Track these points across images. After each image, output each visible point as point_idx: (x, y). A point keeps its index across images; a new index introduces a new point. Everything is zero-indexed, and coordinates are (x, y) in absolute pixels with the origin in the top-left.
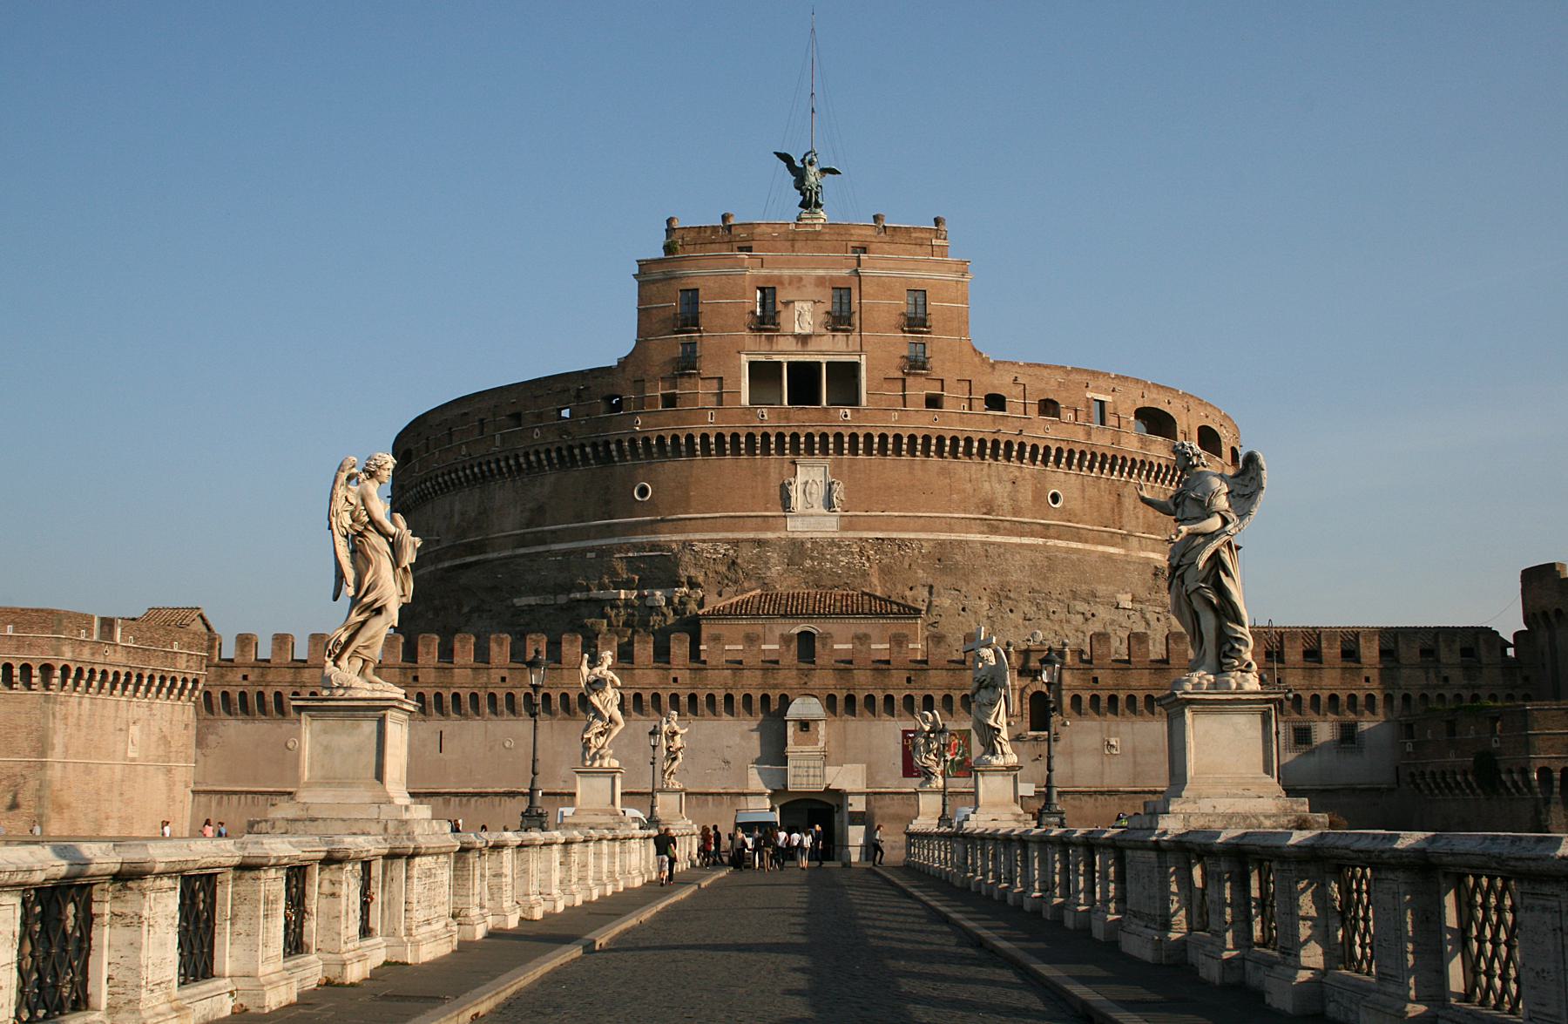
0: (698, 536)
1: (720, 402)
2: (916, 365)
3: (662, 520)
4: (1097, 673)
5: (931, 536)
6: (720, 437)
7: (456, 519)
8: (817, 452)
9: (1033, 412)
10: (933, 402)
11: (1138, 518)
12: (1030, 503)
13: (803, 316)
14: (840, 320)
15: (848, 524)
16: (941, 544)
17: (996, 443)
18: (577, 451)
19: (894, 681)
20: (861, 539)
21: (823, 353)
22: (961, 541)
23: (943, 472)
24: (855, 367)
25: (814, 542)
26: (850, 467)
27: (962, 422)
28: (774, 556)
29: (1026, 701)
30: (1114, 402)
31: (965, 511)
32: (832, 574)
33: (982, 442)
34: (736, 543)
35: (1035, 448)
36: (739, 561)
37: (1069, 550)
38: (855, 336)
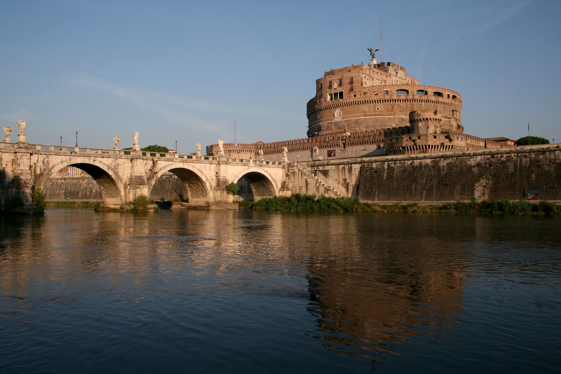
1: (325, 101)
2: (352, 90)
4: (351, 139)
10: (355, 96)
11: (398, 110)
13: (335, 85)
14: (340, 85)
15: (343, 118)
16: (356, 120)
21: (338, 91)
24: (342, 92)
25: (338, 121)
27: (359, 99)
28: (333, 125)
30: (391, 90)
31: (361, 113)
34: (328, 123)
38: (342, 87)
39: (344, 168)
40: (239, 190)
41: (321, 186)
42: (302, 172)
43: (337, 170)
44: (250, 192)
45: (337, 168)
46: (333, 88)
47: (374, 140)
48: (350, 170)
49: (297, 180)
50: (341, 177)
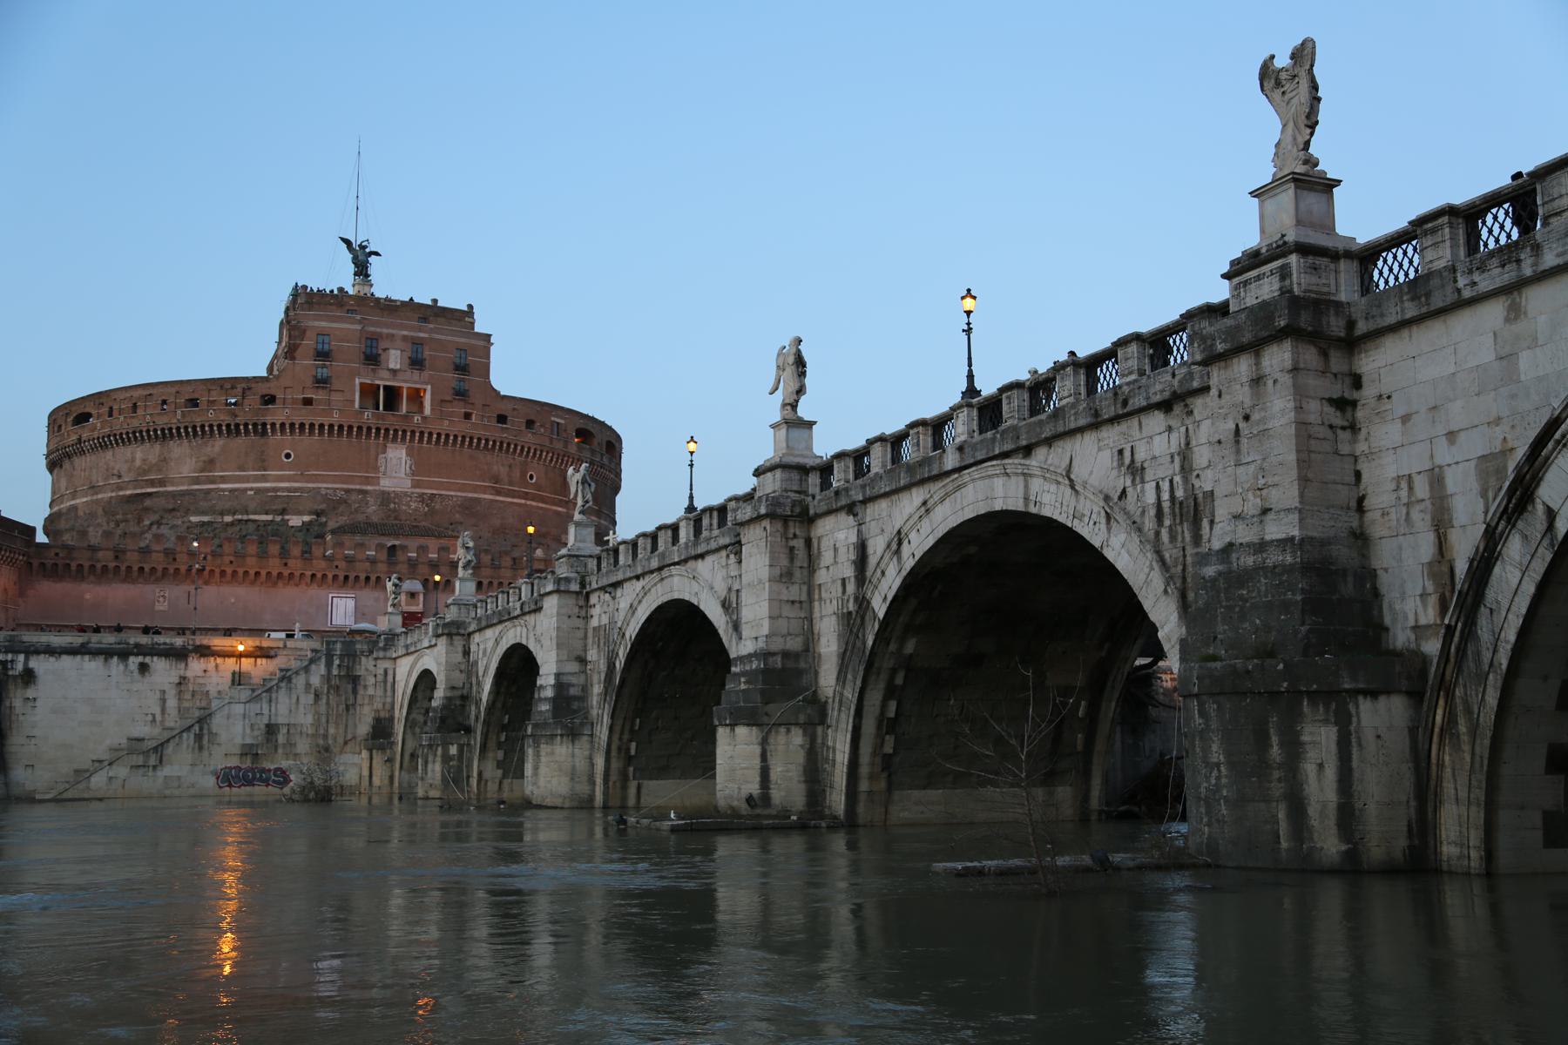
2: (461, 394)
3: (302, 474)
5: (464, 494)
6: (341, 427)
7: (138, 463)
9: (523, 428)
10: (467, 416)
13: (395, 359)
14: (416, 363)
15: (416, 484)
17: (502, 443)
18: (242, 427)
20: (423, 494)
21: (405, 381)
31: (484, 481)
33: (494, 442)
34: (348, 491)
35: (523, 448)
37: (538, 507)
40: (249, 741)
44: (327, 749)
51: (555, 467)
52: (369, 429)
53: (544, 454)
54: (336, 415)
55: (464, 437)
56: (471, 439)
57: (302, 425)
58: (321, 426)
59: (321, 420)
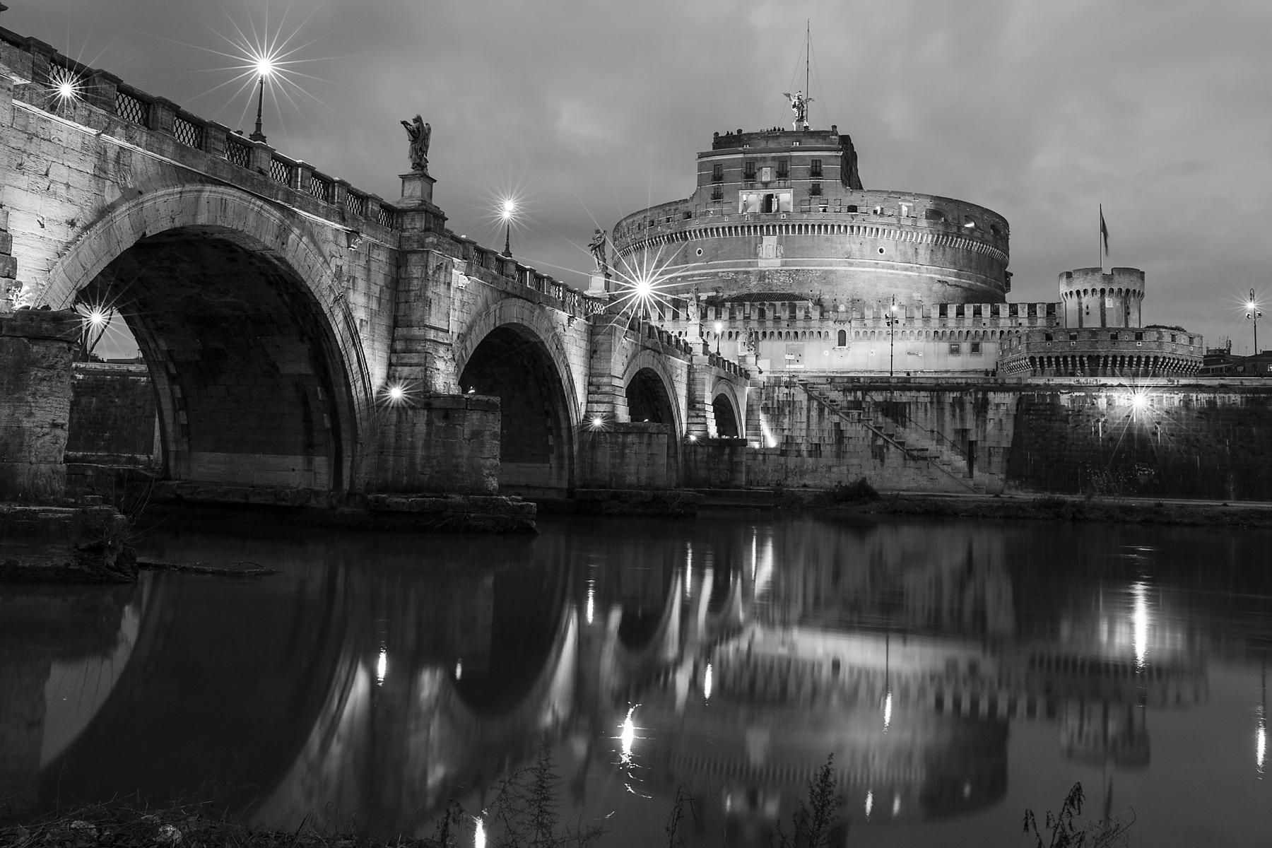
0: (721, 270)
5: (822, 268)
6: (730, 228)
8: (771, 233)
12: (868, 253)
13: (766, 174)
14: (782, 174)
19: (782, 326)
22: (835, 270)
23: (827, 240)
26: (786, 239)
28: (752, 278)
29: (837, 333)
30: (914, 206)
32: (776, 285)
33: (846, 227)
34: (736, 273)
36: (738, 280)
37: (887, 273)
39: (959, 403)
41: (892, 447)
42: (820, 403)
43: (935, 406)
45: (935, 400)
46: (758, 180)
47: (940, 331)
48: (982, 408)
49: (804, 426)
50: (950, 426)
51: (905, 240)
52: (749, 227)
53: (892, 232)
54: (726, 219)
55: (820, 226)
56: (826, 226)
57: (706, 230)
58: (717, 229)
59: (717, 225)
